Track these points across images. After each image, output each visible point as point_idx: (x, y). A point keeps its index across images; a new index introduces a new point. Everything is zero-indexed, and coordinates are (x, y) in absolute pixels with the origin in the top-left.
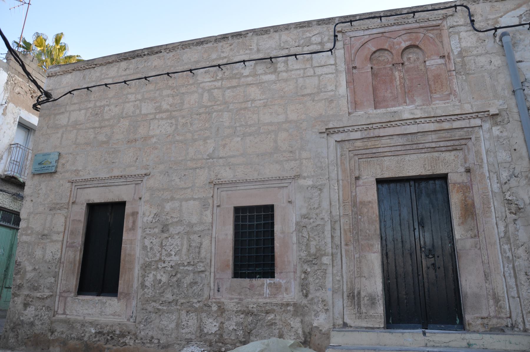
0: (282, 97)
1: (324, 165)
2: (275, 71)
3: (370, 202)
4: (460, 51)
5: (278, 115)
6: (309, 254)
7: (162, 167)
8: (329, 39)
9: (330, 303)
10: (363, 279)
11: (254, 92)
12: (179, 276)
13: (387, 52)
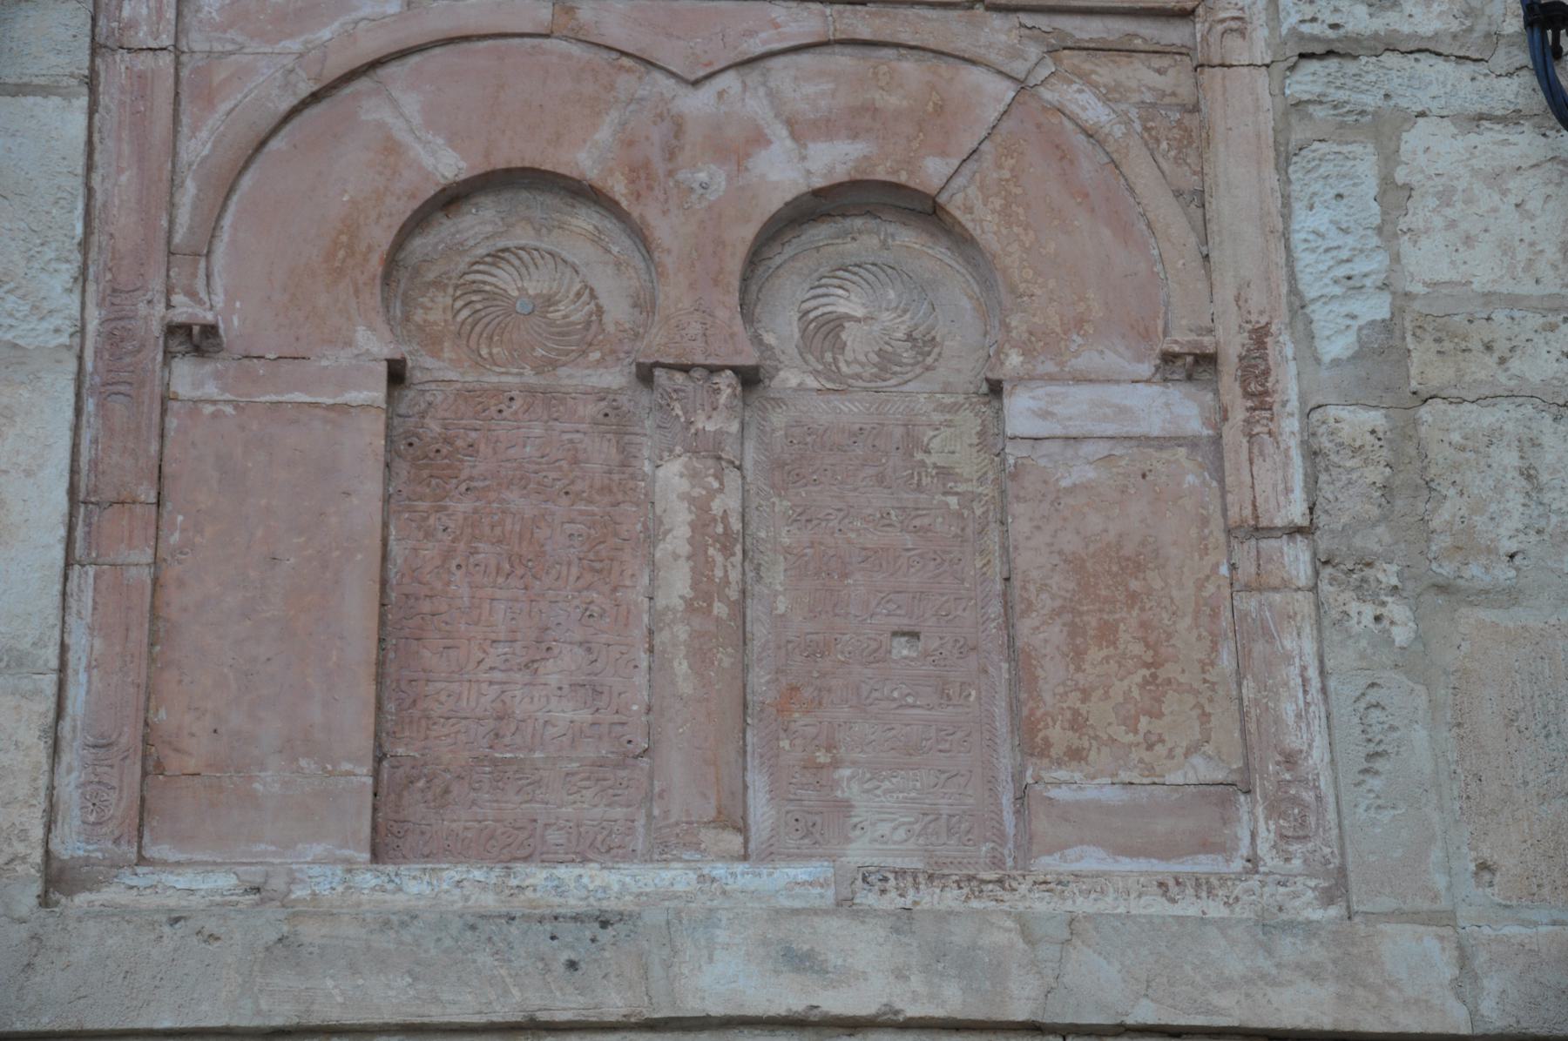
13: (585, 219)
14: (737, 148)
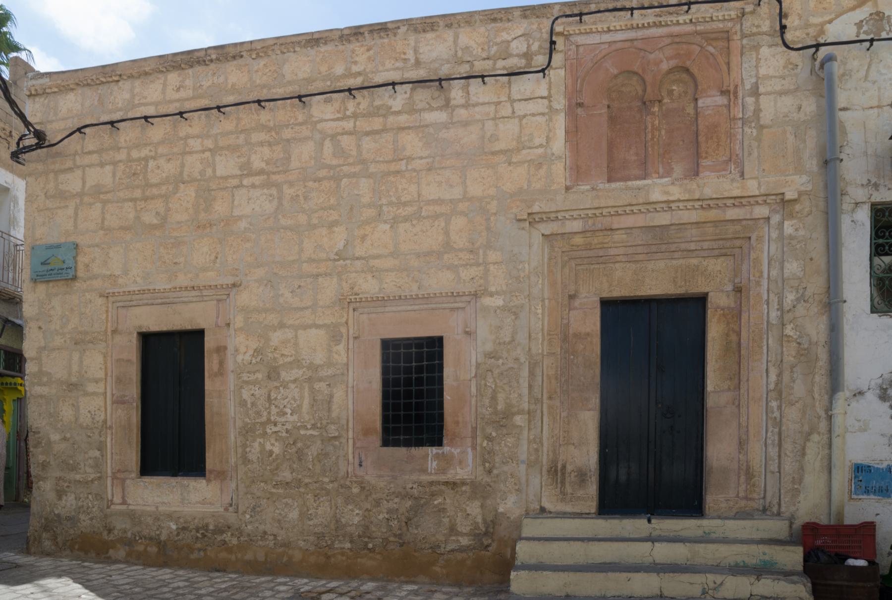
1: (522, 275)
2: (447, 105)
4: (756, 83)
5: (451, 186)
8: (540, 47)
13: (635, 78)
14: (658, 63)
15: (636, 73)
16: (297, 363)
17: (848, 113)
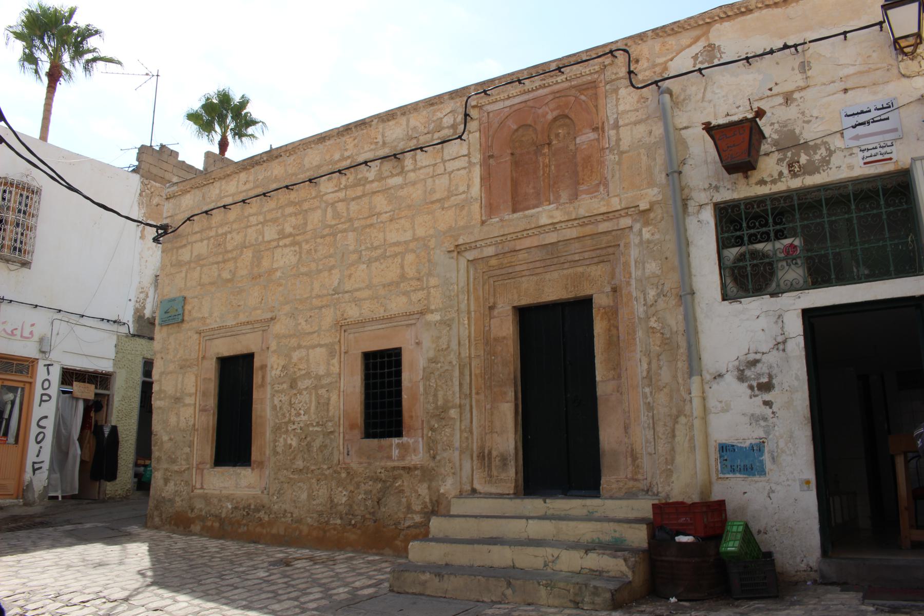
0: (409, 207)
1: (453, 294)
2: (402, 172)
3: (504, 338)
6: (437, 408)
7: (287, 308)
9: (458, 464)
10: (495, 435)
11: (380, 202)
12: (308, 439)
15: (530, 126)
16: (308, 375)
17: (689, 130)
